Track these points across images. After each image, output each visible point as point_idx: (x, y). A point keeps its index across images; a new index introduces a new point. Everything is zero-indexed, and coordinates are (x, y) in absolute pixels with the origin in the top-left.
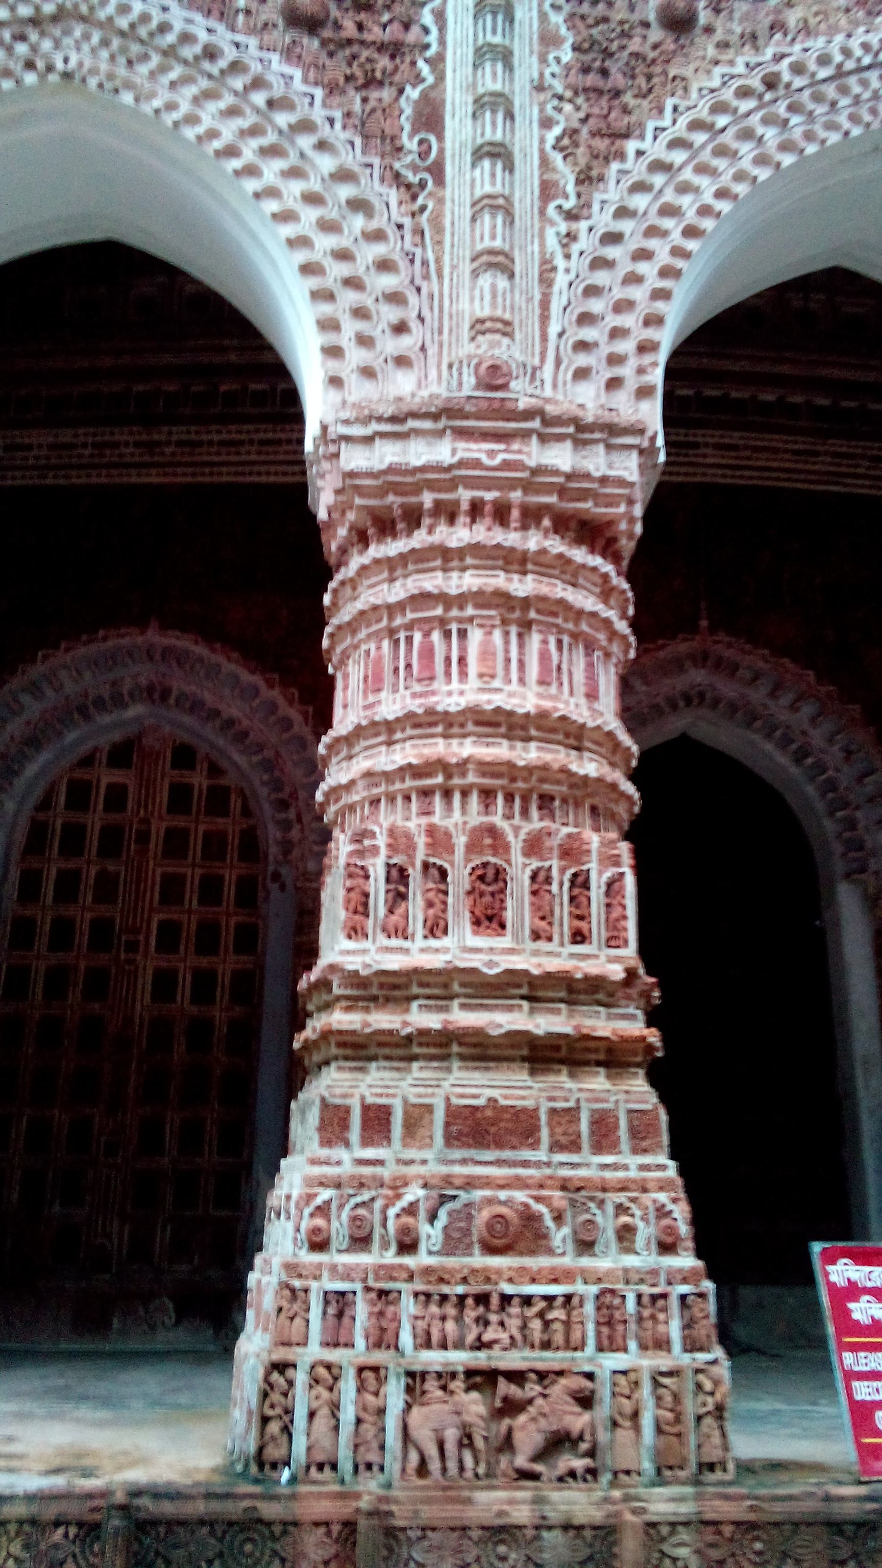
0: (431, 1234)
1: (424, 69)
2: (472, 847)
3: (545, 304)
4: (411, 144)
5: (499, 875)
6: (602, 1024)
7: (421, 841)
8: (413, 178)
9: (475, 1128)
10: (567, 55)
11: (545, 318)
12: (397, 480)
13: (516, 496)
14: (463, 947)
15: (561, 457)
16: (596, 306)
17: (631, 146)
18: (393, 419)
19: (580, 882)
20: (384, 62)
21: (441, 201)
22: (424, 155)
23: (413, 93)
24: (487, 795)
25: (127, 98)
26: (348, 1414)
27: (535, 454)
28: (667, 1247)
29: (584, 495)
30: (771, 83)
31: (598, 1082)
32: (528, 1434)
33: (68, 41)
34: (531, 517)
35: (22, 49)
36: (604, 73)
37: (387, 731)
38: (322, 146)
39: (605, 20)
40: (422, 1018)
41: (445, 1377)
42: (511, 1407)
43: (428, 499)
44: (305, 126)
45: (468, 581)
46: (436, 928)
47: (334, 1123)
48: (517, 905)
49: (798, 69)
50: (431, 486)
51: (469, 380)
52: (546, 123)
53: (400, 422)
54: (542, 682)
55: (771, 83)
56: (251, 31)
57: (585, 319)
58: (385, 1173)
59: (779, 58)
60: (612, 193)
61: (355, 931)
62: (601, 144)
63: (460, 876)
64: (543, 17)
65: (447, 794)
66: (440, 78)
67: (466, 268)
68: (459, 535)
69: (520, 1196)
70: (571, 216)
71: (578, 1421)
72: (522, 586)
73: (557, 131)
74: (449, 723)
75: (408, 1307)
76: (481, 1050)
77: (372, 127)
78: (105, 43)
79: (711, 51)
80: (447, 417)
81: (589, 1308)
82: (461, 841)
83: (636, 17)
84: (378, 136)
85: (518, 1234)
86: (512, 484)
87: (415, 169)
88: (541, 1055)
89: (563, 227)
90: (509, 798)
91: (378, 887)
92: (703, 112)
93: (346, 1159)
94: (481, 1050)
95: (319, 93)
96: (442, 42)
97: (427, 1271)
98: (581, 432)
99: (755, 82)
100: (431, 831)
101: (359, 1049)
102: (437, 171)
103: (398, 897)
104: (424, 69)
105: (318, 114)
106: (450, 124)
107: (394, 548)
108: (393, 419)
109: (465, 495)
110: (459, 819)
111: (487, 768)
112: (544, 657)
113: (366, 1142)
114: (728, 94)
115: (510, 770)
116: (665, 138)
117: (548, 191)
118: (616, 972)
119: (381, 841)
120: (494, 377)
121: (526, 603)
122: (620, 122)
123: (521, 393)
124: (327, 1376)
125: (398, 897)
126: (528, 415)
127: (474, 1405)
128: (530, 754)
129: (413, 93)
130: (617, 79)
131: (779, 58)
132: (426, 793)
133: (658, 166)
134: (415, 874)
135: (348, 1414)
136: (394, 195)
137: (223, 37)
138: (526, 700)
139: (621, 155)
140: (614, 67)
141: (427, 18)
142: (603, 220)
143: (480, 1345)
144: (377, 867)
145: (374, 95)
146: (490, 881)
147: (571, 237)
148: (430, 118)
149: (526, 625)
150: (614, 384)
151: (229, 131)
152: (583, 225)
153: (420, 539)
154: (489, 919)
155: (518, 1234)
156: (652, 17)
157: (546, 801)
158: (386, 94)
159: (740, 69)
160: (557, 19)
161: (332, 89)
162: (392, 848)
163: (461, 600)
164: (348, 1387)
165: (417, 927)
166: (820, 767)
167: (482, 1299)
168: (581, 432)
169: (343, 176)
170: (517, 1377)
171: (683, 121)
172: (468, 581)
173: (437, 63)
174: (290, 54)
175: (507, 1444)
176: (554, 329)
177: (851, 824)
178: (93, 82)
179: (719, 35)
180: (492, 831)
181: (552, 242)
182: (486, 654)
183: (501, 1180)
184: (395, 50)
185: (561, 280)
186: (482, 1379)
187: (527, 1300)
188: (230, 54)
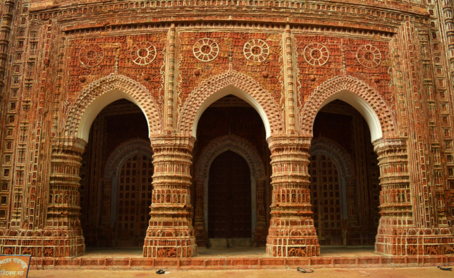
0: (161, 235)
1: (162, 85)
2: (167, 192)
3: (177, 120)
4: (160, 97)
5: (170, 196)
6: (180, 212)
7: (161, 192)
8: (160, 102)
9: (166, 224)
10: (181, 81)
11: (177, 122)
12: (158, 145)
13: (173, 147)
14: (166, 204)
15: (178, 142)
16: (184, 120)
17: (189, 95)
18: (158, 138)
19: (179, 196)
20: (157, 84)
21: (164, 106)
22: (162, 99)
23: (160, 89)
24: (169, 186)
25: (124, 91)
26: (152, 252)
27: (174, 142)
28: (186, 235)
29: (181, 146)
30: (209, 83)
31: (180, 219)
32: (169, 253)
33: (117, 83)
34: (175, 149)
35: (110, 85)
36: (186, 83)
37: (158, 178)
38: (149, 98)
39: (187, 75)
40: (161, 212)
41: (161, 248)
42: (168, 251)
43: (162, 148)
44: (146, 95)
45: (167, 159)
46: (163, 202)
47: (152, 223)
48: (172, 199)
49: (213, 80)
50: (163, 146)
51: (166, 133)
52: (178, 93)
53: (159, 138)
54: (176, 171)
55: (209, 83)
56: (139, 81)
57: (182, 122)
58: (157, 229)
59: (210, 79)
60: (186, 103)
61: (154, 202)
62: (185, 95)
63: (165, 195)
64: (178, 75)
65: (164, 186)
66: (164, 87)
67: (167, 116)
68: (165, 153)
69: (170, 231)
70: (181, 106)
71: (174, 252)
72: (173, 159)
73: (179, 94)
74: (164, 177)
75: (158, 242)
76: (167, 216)
77: (155, 95)
78: (121, 83)
79: (201, 79)
80: (164, 138)
81: (176, 242)
82: (165, 192)
83: (191, 74)
84: (155, 96)
85: (170, 234)
86: (172, 146)
87: (160, 101)
88: (174, 216)
89: (180, 108)
90: (171, 186)
91: (156, 197)
92: (199, 89)
93: (153, 227)
94: (167, 216)
95: (148, 90)
96: (164, 80)
97: (160, 238)
98: (181, 138)
99: (207, 83)
100: (162, 190)
101: (154, 215)
102: (163, 101)
103: (158, 198)
104: (162, 85)
105: (148, 94)
106: (165, 94)
107: (159, 154)
108: (158, 138)
109: (166, 147)
110: (165, 189)
111: (168, 183)
112: (176, 168)
113: (155, 225)
114: (203, 86)
115: (171, 183)
116: (194, 93)
117: (178, 103)
118: (183, 206)
119: (157, 192)
120: (169, 132)
121: (174, 161)
122: (188, 91)
123: (173, 135)
124: (150, 248)
125: (158, 198)
126: (174, 137)
127: (164, 251)
128: (174, 181)
129: (160, 89)
130: (188, 85)
131: (210, 79)
132: (162, 186)
133: (193, 98)
134: (160, 195)
135: (152, 252)
136: (158, 105)
137: (136, 83)
138: (174, 174)
139: (188, 97)
140: (187, 83)
141: (163, 77)
142: (185, 107)
143: (165, 245)
144: (156, 194)
145: (156, 90)
146: (169, 196)
147: (181, 110)
148: (163, 93)
149: (174, 164)
150: (186, 130)
151: (137, 95)
152: (182, 108)
153: (162, 153)
154: (168, 201)
155: (170, 234)
156: (194, 73)
157: (176, 186)
158: (157, 89)
159: (205, 81)
160: (180, 75)
161: (150, 90)
162: (158, 193)
163: (166, 161)
164: (152, 249)
165: (161, 201)
166: (249, 156)
167: (165, 241)
168: (181, 138)
169: (151, 102)
170: (169, 248)
171: (197, 90)
172: (167, 159)
173: (164, 84)
174: (144, 84)
175: (168, 254)
176: (178, 124)
177: (253, 166)
178: (120, 89)
179: (203, 76)
180: (169, 190)
181: (178, 111)
182: (169, 168)
183: (168, 229)
184: (158, 82)
185: (179, 116)
186: (165, 248)
187: (170, 241)
188: (137, 85)
